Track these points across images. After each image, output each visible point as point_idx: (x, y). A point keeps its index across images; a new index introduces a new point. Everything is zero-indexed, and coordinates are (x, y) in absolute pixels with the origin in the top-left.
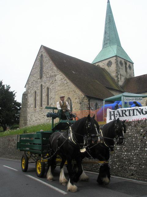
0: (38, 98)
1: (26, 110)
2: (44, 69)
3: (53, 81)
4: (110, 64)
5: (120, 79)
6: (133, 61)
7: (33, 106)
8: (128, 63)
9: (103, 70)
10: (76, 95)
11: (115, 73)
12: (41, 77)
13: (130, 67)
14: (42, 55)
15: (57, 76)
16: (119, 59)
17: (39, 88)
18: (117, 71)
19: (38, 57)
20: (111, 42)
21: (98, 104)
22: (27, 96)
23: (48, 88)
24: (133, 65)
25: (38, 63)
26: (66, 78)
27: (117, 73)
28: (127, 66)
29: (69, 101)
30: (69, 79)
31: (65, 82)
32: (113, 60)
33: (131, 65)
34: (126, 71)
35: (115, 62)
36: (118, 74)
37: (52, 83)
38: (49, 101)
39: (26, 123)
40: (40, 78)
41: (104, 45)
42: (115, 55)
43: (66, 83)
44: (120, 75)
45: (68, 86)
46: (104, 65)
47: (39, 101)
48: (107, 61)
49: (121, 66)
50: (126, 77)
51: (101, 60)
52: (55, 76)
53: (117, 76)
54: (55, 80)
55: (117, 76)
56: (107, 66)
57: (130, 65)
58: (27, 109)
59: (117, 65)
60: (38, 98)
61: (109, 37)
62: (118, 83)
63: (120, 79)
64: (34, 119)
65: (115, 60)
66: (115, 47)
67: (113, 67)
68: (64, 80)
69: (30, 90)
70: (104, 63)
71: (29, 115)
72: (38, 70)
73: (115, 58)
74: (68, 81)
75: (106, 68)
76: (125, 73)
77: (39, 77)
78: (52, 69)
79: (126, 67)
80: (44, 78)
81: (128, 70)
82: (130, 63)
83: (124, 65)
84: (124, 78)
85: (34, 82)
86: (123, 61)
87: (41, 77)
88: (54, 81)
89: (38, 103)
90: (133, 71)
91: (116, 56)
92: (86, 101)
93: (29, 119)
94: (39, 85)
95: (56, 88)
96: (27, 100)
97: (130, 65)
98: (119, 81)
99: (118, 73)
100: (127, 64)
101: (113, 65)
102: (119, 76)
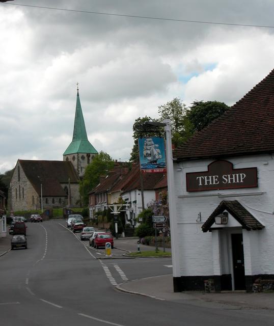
0: (18, 193)
4: (74, 158)
8: (91, 155)
12: (19, 181)
16: (80, 155)
17: (18, 187)
44: (81, 168)
59: (78, 160)
60: (18, 193)
66: (79, 143)
67: (76, 160)
73: (77, 154)
83: (86, 158)
87: (19, 181)
89: (18, 196)
94: (18, 185)
102: (80, 169)
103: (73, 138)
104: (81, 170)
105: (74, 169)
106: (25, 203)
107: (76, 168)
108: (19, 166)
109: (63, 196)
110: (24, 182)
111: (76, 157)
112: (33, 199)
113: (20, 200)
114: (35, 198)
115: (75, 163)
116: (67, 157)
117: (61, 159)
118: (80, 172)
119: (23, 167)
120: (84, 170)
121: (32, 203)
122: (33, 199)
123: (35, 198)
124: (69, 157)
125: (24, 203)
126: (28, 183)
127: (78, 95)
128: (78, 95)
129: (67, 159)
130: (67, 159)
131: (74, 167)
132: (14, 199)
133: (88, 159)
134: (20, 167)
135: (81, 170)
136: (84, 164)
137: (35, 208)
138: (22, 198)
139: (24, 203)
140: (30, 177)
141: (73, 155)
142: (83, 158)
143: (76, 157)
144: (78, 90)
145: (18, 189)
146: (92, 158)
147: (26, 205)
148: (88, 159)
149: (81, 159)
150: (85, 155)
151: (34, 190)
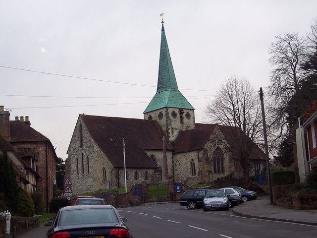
0: (80, 165)
2: (83, 139)
4: (161, 116)
5: (171, 133)
8: (185, 112)
9: (156, 121)
12: (81, 146)
13: (188, 116)
14: (81, 125)
16: (170, 111)
17: (80, 156)
22: (70, 162)
23: (88, 157)
24: (193, 112)
25: (78, 132)
27: (167, 127)
28: (184, 116)
30: (105, 153)
33: (190, 112)
34: (182, 122)
36: (169, 129)
37: (91, 153)
38: (90, 169)
44: (172, 129)
48: (158, 112)
53: (167, 131)
57: (188, 113)
59: (168, 117)
60: (80, 165)
63: (171, 133)
66: (167, 94)
67: (164, 118)
73: (165, 110)
75: (158, 121)
78: (90, 140)
80: (84, 148)
81: (185, 120)
82: (188, 111)
83: (179, 115)
85: (76, 150)
86: (177, 111)
87: (81, 146)
89: (80, 171)
90: (194, 118)
91: (166, 107)
94: (80, 154)
97: (188, 113)
100: (186, 112)
101: (164, 117)
102: (170, 131)
103: (158, 88)
104: (172, 133)
105: (162, 131)
106: (91, 180)
107: (164, 129)
108: (81, 125)
109: (150, 168)
110: (90, 147)
111: (164, 113)
112: (105, 173)
113: (83, 177)
114: (108, 171)
115: (163, 122)
116: (150, 116)
117: (142, 117)
118: (171, 135)
119: (87, 125)
120: (176, 133)
121: (102, 179)
122: (105, 173)
123: (108, 171)
124: (153, 115)
125: (90, 181)
126: (96, 148)
127: (163, 29)
128: (163, 29)
129: (150, 117)
130: (150, 117)
131: (161, 128)
132: (73, 176)
133: (182, 118)
134: (83, 124)
135: (172, 133)
136: (176, 124)
137: (108, 187)
138: (85, 174)
139: (90, 181)
140: (100, 140)
141: (161, 111)
142: (174, 114)
143: (164, 113)
144: (163, 22)
145: (80, 160)
146: (186, 115)
147: (93, 184)
148: (182, 118)
149: (171, 117)
150: (177, 111)
151: (106, 158)
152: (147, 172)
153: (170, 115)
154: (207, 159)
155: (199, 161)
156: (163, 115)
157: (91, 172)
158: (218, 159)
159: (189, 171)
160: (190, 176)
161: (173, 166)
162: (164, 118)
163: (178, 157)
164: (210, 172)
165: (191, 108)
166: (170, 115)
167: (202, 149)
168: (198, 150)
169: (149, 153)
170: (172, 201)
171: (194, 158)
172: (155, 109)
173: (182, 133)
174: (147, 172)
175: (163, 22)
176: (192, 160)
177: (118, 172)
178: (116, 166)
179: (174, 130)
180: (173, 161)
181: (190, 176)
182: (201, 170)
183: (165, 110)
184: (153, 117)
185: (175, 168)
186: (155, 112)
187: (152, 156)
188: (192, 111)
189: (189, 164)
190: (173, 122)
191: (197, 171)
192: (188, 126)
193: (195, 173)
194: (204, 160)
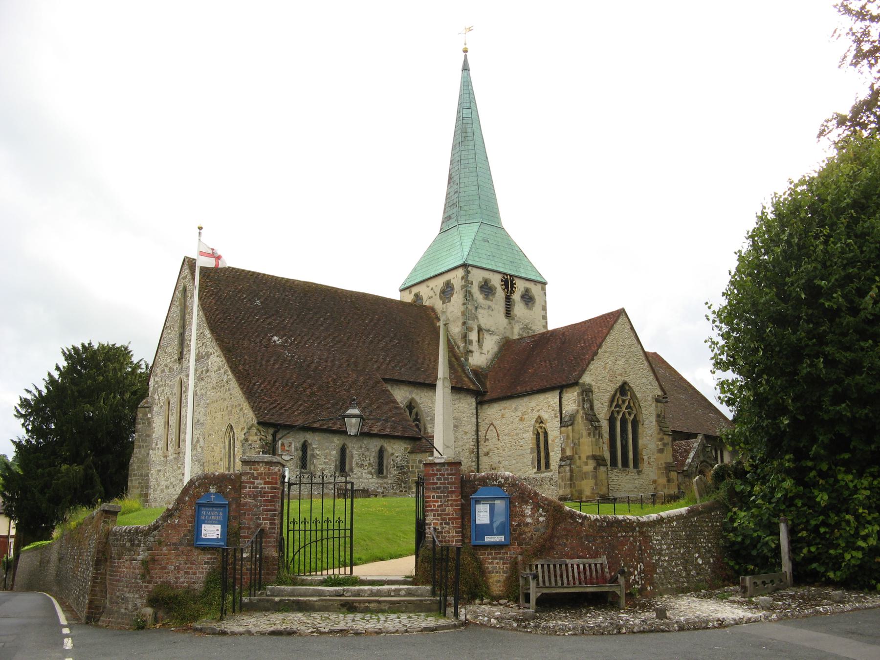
1: (148, 454)
3: (202, 372)
4: (447, 292)
5: (475, 343)
6: (546, 276)
7: (161, 444)
8: (520, 286)
9: (433, 309)
10: (242, 420)
11: (460, 324)
13: (528, 299)
15: (211, 357)
16: (477, 277)
17: (176, 390)
18: (467, 317)
19: (177, 292)
20: (462, 213)
21: (311, 444)
22: (151, 412)
24: (544, 289)
25: (176, 310)
26: (226, 367)
27: (464, 323)
28: (516, 297)
29: (231, 435)
31: (225, 378)
32: (456, 278)
33: (535, 290)
34: (508, 313)
35: (463, 287)
36: (469, 329)
39: (147, 495)
40: (179, 360)
41: (443, 222)
42: (461, 262)
43: (227, 382)
44: (480, 330)
45: (229, 390)
46: (432, 294)
47: (174, 430)
48: (440, 283)
49: (487, 297)
50: (508, 334)
51: (424, 278)
52: (208, 355)
53: (465, 337)
54: (207, 371)
55: (465, 337)
56: (441, 298)
57: (527, 291)
58: (151, 452)
59: (468, 295)
61: (457, 195)
62: (467, 360)
64: (163, 483)
65: (462, 278)
66: (468, 233)
67: (457, 298)
68: (222, 371)
69: (158, 395)
70: (432, 289)
71: (153, 471)
72: (174, 334)
73: (460, 272)
74: (231, 376)
75: (438, 305)
76: (502, 321)
77: (176, 357)
79: (508, 299)
81: (519, 309)
83: (500, 293)
84: (496, 338)
88: (204, 373)
90: (544, 308)
91: (464, 266)
92: (255, 438)
93: (152, 482)
94: (175, 382)
95: (209, 393)
96: (149, 423)
97: (527, 291)
98: (471, 352)
99: (470, 323)
101: (455, 296)
102: (473, 336)
103: (447, 219)
118: (474, 347)
120: (491, 345)
127: (466, 68)
128: (466, 68)
142: (487, 289)
144: (465, 51)
145: (174, 400)
146: (523, 297)
150: (496, 281)
152: (381, 453)
153: (475, 290)
154: (592, 418)
155: (563, 423)
156: (452, 289)
157: (198, 441)
158: (624, 421)
159: (529, 457)
160: (531, 472)
161: (478, 442)
162: (457, 298)
163: (493, 412)
164: (599, 461)
165: (539, 279)
166: (475, 290)
167: (576, 384)
168: (561, 388)
169: (401, 395)
170: (440, 609)
171: (545, 416)
172: (432, 274)
173: (507, 346)
174: (381, 453)
175: (465, 51)
176: (540, 420)
177: (274, 440)
178: (268, 419)
179: (487, 336)
180: (477, 425)
181: (531, 472)
182: (569, 453)
183: (460, 272)
184: (425, 298)
185: (483, 449)
186: (432, 284)
187: (411, 406)
188: (539, 286)
189: (529, 436)
190: (479, 310)
191: (555, 457)
192: (526, 328)
193: (547, 466)
194: (580, 421)
